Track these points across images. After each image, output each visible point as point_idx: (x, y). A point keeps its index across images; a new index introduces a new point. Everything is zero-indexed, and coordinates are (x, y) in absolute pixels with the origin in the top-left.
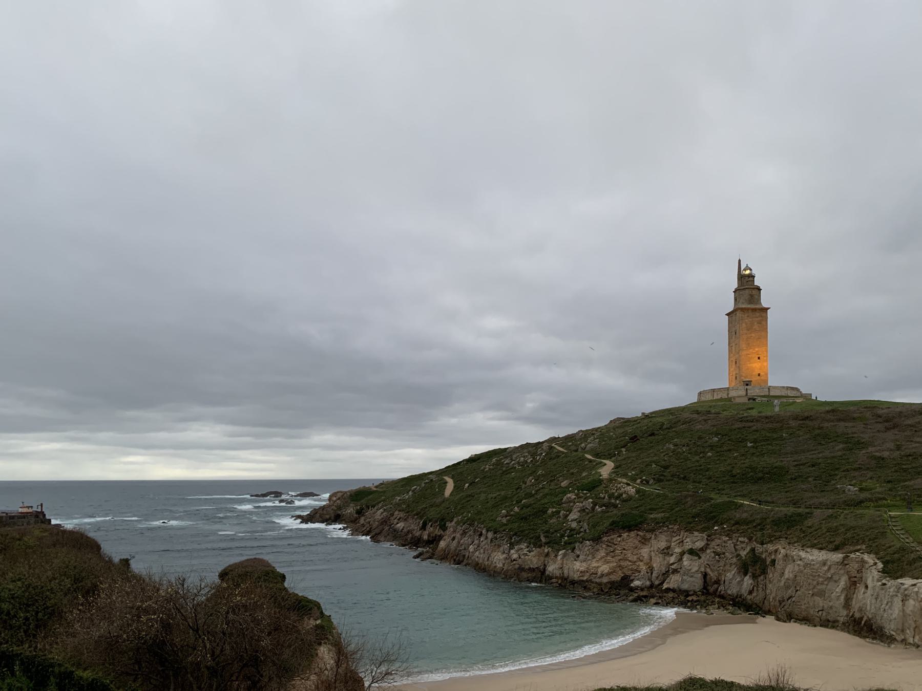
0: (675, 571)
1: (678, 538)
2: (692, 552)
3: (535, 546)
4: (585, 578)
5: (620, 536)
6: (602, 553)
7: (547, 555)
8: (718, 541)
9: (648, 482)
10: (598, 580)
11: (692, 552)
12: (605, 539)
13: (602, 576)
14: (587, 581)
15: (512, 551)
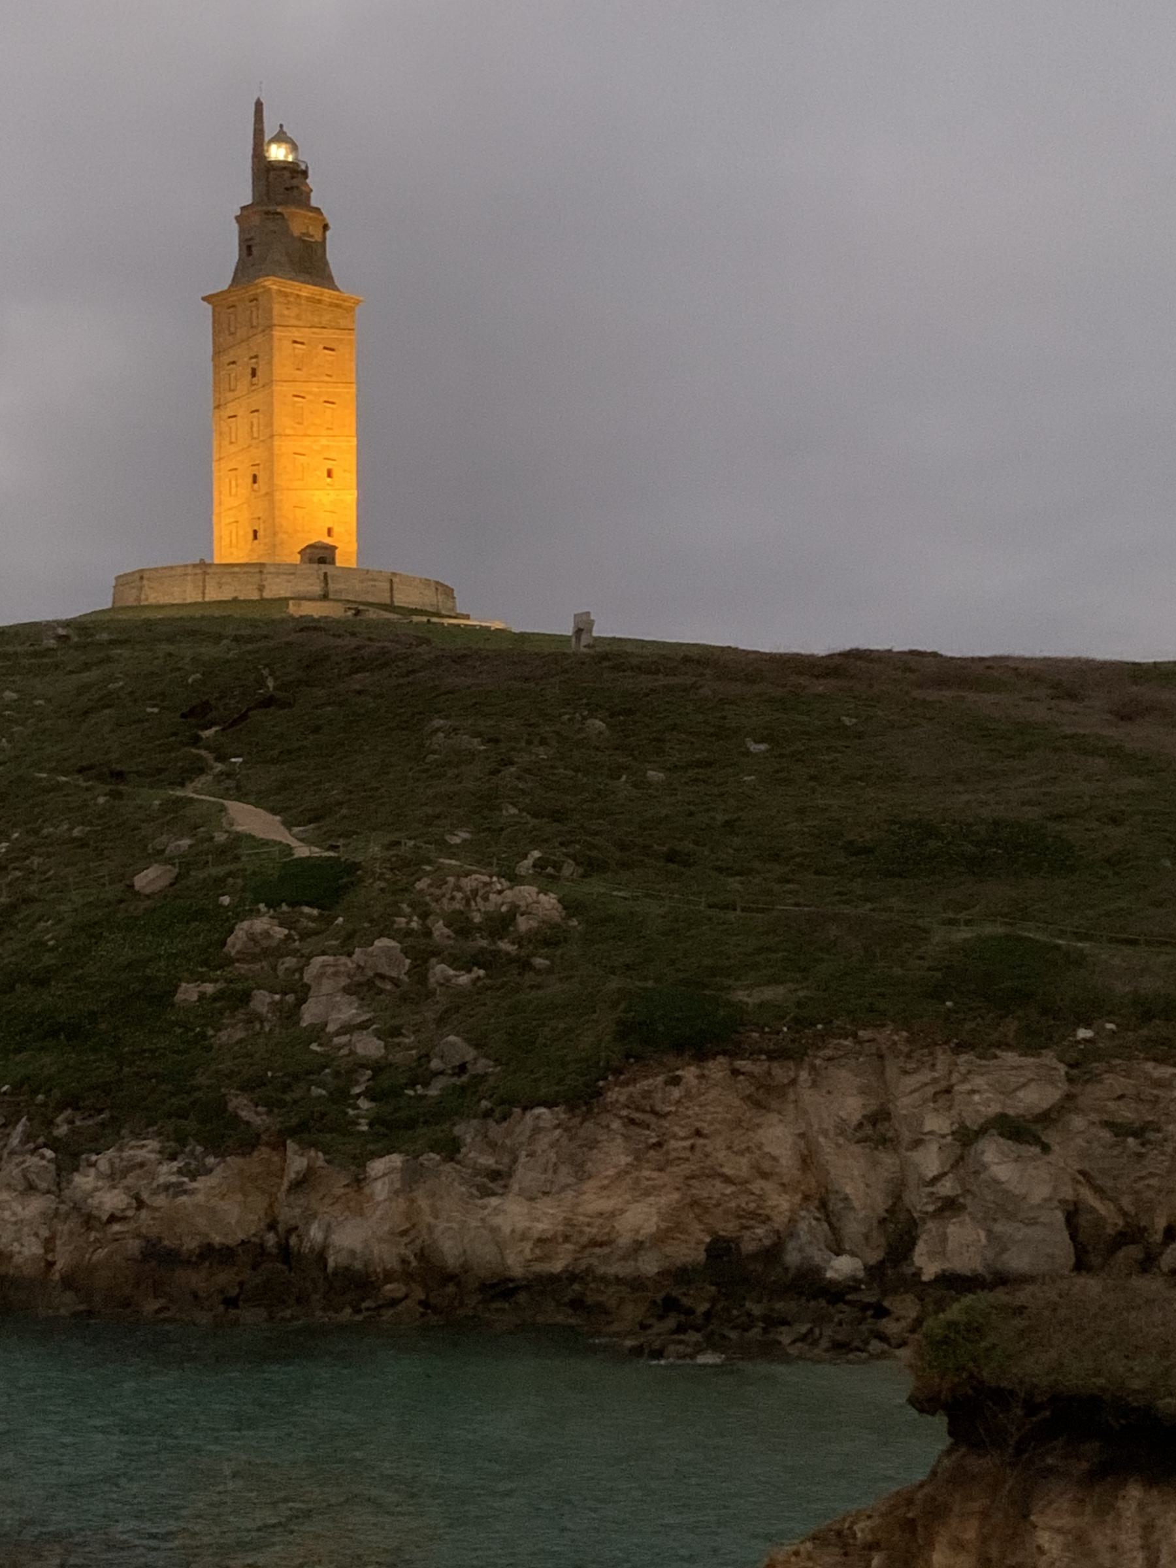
0: (950, 1207)
1: (925, 1076)
2: (1016, 1130)
3: (216, 1146)
5: (676, 1081)
8: (1115, 1082)
9: (557, 866)
11: (1016, 1130)
15: (84, 1181)
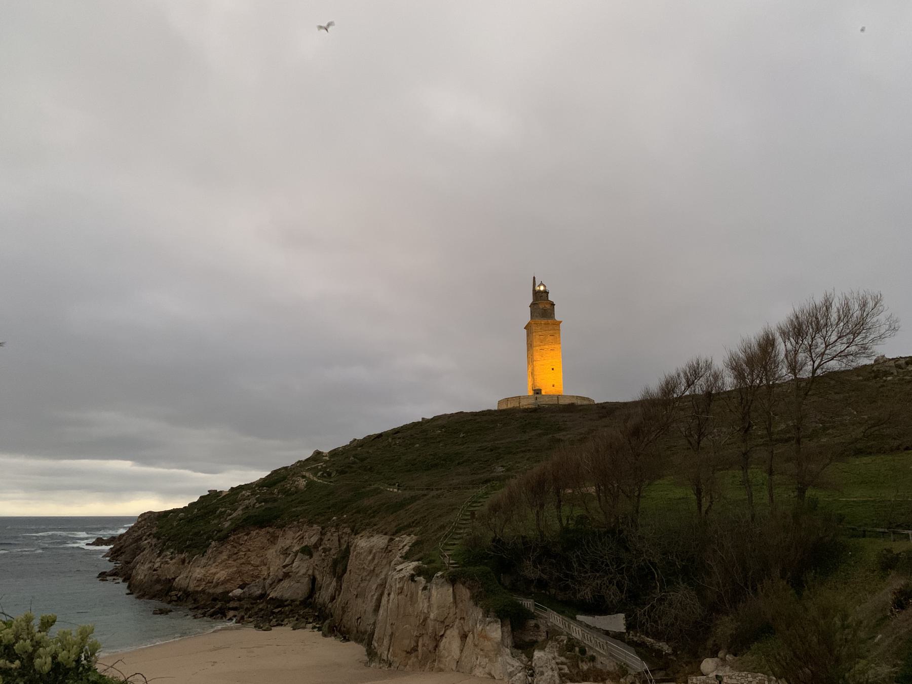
5: (247, 534)
6: (224, 556)
7: (183, 561)
10: (211, 591)
12: (232, 538)
13: (217, 584)
14: (200, 592)
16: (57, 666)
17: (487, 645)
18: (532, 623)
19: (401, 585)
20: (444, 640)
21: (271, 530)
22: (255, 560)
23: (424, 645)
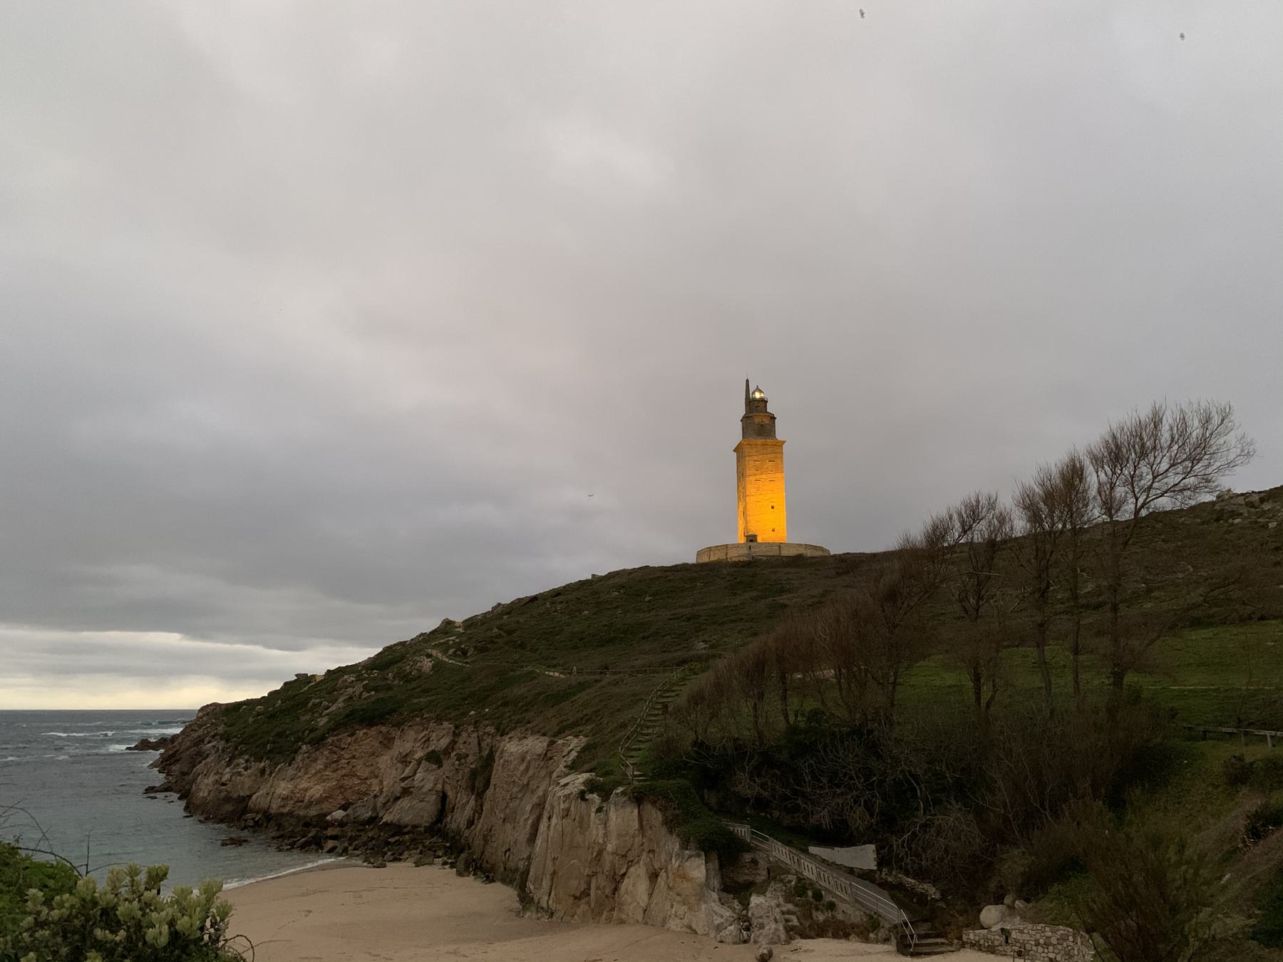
4: (286, 810)
7: (263, 772)
10: (302, 813)
12: (330, 740)
13: (310, 804)
14: (287, 814)
16: (175, 935)
17: (686, 887)
18: (747, 857)
19: (566, 805)
20: (626, 881)
21: (384, 729)
22: (362, 771)
23: (598, 888)
